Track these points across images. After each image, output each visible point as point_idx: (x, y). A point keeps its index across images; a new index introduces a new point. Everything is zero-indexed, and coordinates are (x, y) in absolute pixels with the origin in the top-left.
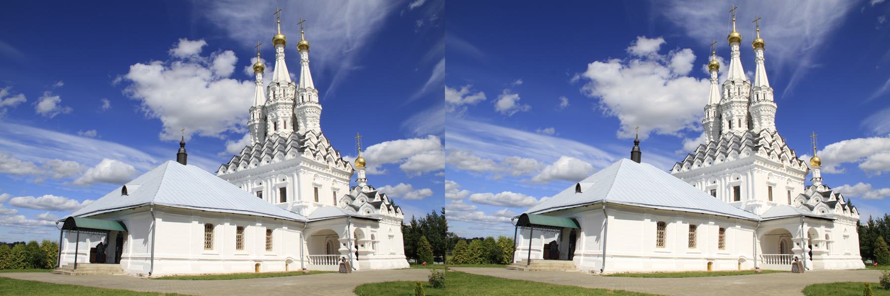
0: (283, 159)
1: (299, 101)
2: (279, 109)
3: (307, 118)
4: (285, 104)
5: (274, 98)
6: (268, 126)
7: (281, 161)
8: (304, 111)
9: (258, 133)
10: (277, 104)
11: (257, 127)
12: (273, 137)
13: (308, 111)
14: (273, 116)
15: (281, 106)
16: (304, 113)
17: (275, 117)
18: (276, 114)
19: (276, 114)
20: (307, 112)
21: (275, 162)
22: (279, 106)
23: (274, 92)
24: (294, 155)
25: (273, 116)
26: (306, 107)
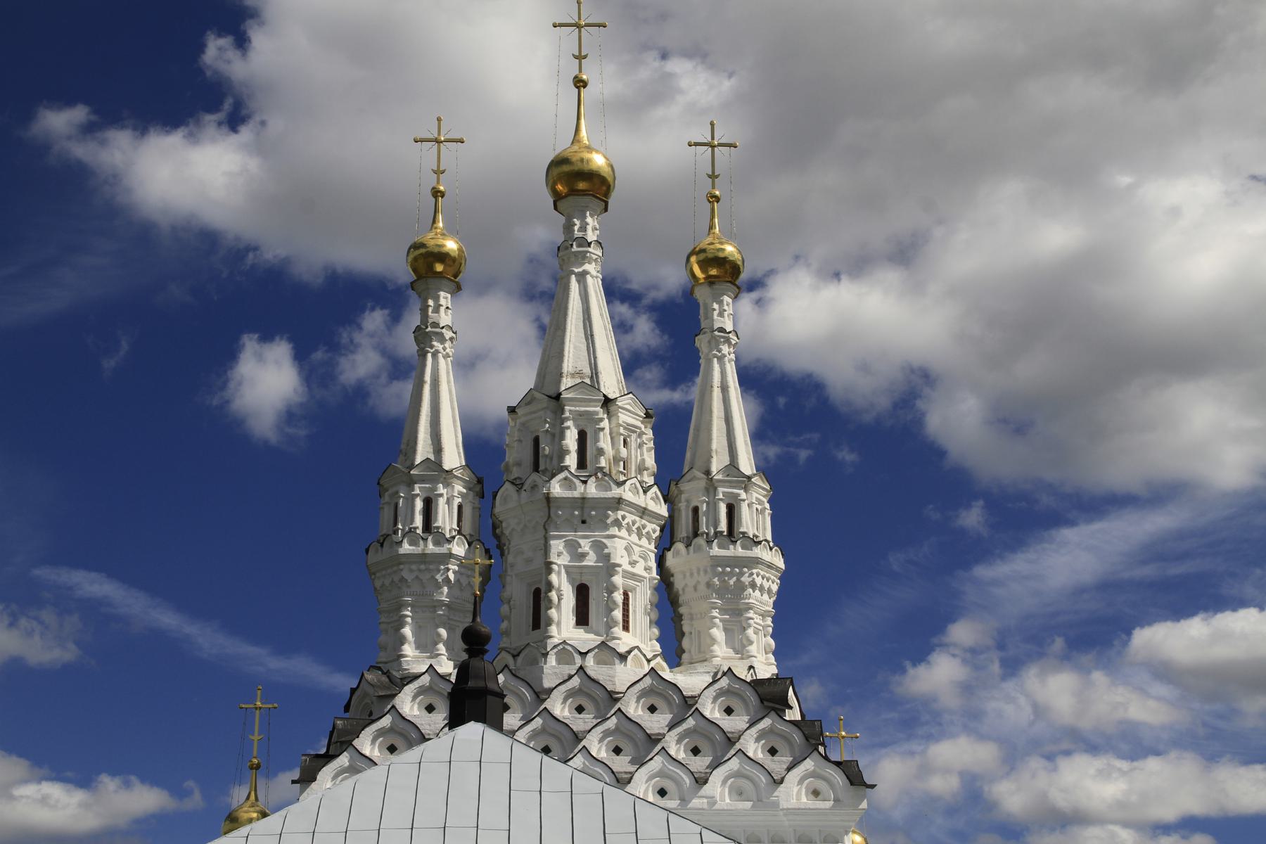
0: (760, 801)
1: (716, 523)
2: (614, 531)
3: (751, 614)
4: (643, 512)
5: (582, 464)
6: (553, 595)
7: (749, 805)
8: (746, 579)
9: (449, 606)
10: (619, 502)
11: (451, 576)
12: (590, 657)
13: (759, 581)
14: (583, 556)
15: (630, 518)
16: (741, 588)
17: (591, 560)
18: (599, 547)
19: (599, 547)
20: (753, 585)
21: (712, 801)
22: (620, 513)
23: (582, 437)
24: (816, 793)
25: (583, 556)
26: (757, 562)
